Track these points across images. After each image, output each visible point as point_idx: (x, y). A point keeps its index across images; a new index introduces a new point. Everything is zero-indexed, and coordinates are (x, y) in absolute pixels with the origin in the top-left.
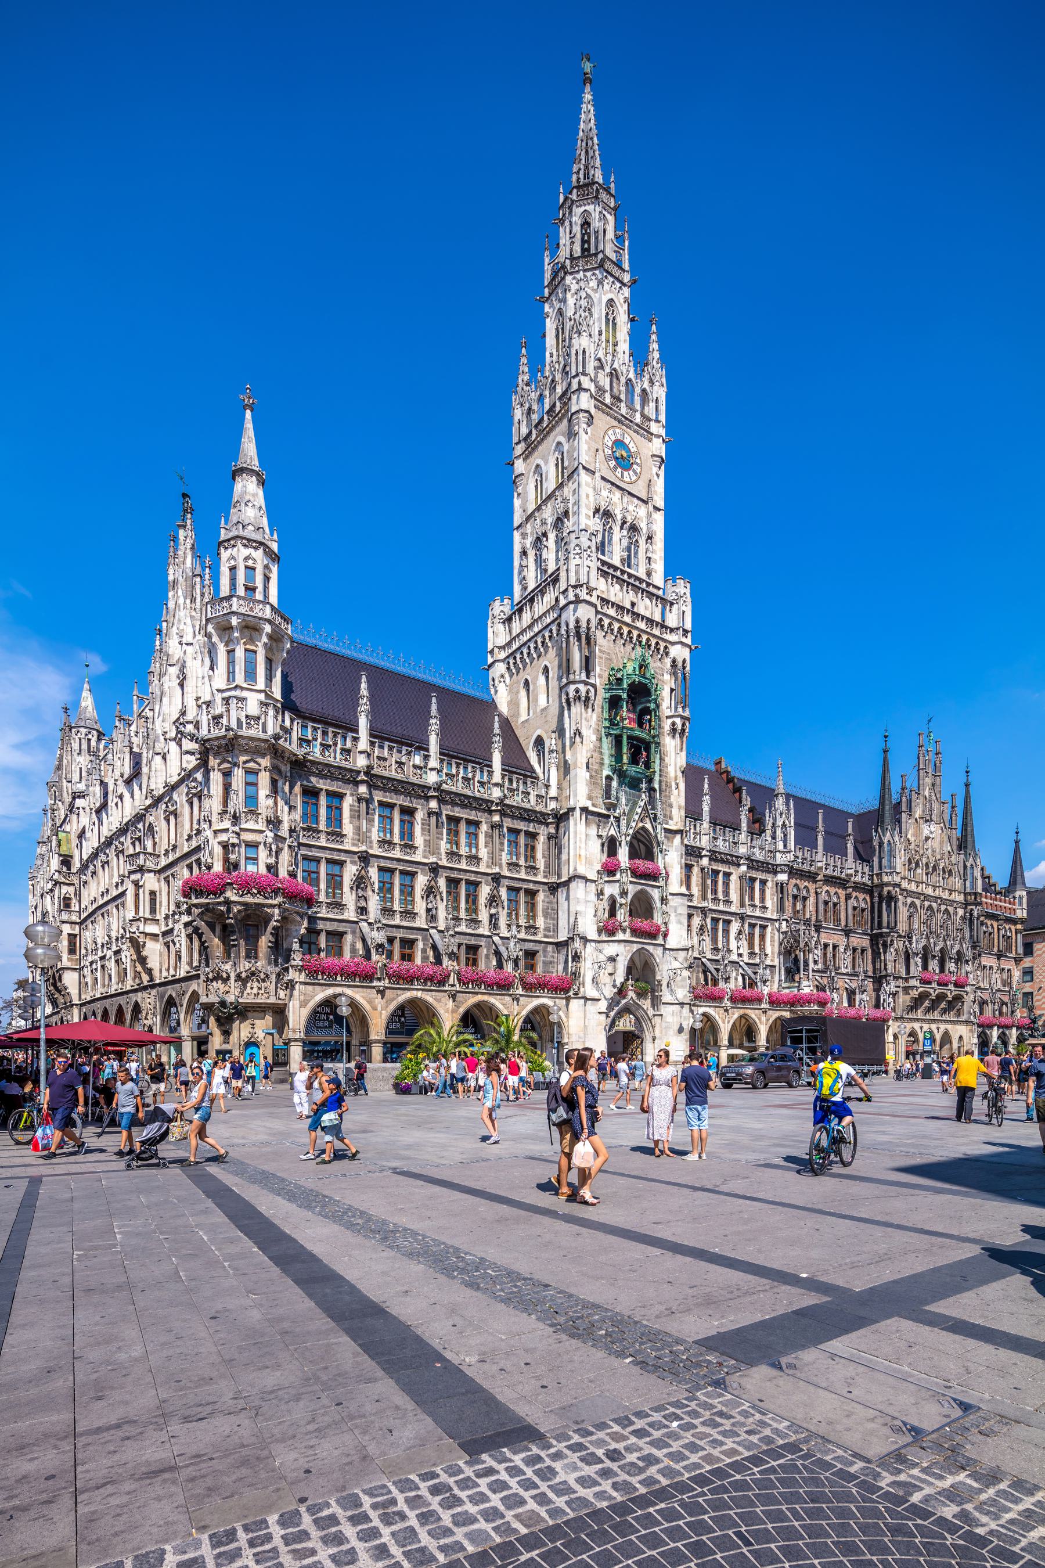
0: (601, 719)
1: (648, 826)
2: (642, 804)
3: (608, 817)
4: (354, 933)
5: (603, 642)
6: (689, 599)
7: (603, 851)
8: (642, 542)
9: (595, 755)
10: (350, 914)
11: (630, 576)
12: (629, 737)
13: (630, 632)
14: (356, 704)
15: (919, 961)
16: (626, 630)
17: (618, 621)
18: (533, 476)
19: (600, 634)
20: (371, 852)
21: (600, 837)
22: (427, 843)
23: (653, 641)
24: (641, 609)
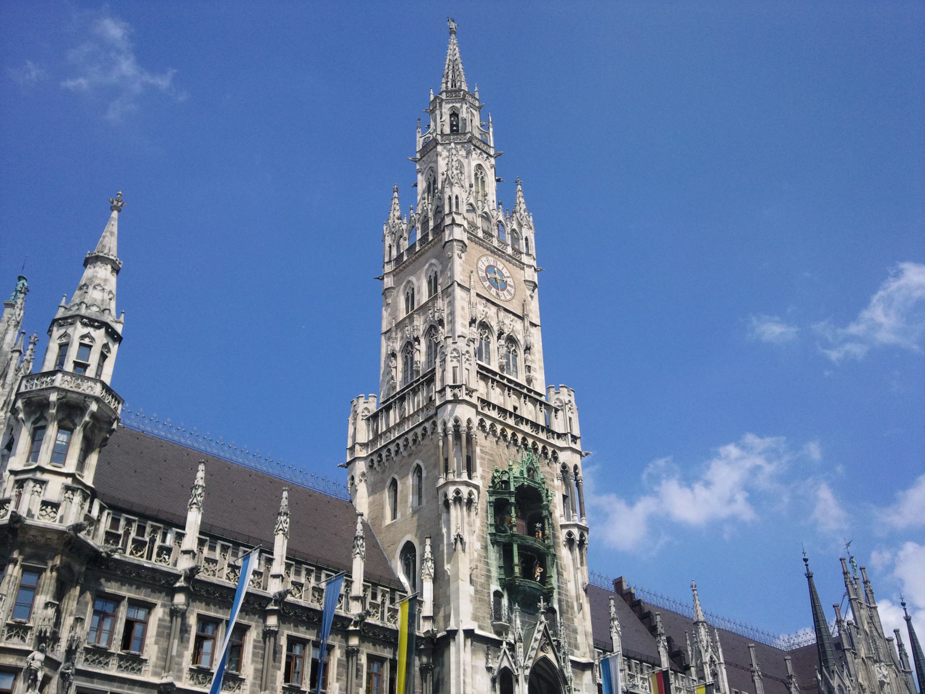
1: (551, 656)
2: (542, 628)
3: (501, 643)
5: (483, 444)
6: (575, 407)
7: (494, 687)
8: (521, 352)
9: (481, 565)
11: (510, 381)
13: (514, 435)
16: (509, 432)
17: (501, 423)
20: (179, 685)
21: (489, 669)
23: (540, 446)
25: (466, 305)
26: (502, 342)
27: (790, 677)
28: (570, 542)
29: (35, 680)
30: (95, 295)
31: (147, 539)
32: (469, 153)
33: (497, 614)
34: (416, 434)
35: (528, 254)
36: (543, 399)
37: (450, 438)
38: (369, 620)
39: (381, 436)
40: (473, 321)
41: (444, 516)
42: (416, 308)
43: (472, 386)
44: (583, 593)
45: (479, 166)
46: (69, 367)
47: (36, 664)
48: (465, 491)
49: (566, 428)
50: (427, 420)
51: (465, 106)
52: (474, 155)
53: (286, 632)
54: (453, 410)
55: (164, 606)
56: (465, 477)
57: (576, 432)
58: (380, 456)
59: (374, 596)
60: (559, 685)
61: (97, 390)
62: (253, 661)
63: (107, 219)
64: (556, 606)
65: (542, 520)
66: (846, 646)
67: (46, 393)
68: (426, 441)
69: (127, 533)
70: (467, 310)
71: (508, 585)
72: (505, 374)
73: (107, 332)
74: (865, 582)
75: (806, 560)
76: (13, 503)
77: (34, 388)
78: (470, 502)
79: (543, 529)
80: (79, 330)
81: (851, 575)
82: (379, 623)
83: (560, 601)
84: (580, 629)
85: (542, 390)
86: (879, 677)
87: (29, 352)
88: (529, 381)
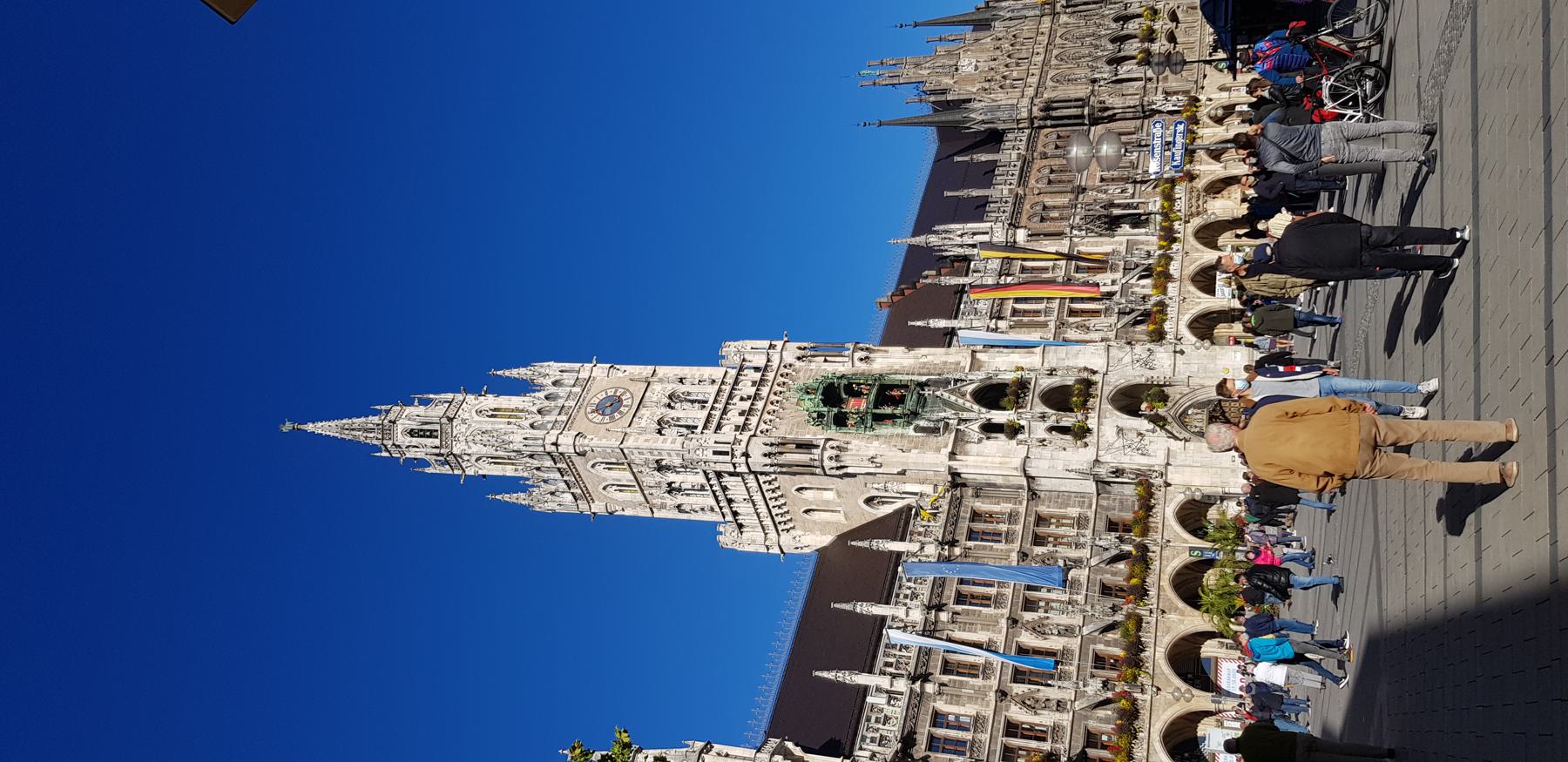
1: (970, 388)
2: (946, 395)
4: (1086, 718)
5: (783, 430)
8: (681, 389)
10: (1065, 719)
11: (715, 401)
14: (843, 685)
16: (770, 407)
18: (614, 497)
19: (775, 433)
21: (980, 440)
22: (985, 627)
24: (752, 391)
25: (642, 438)
33: (934, 431)
36: (733, 372)
40: (660, 432)
45: (479, 412)
56: (817, 451)
66: (942, 98)
70: (648, 436)
72: (709, 405)
84: (944, 359)
85: (721, 371)
86: (970, 69)
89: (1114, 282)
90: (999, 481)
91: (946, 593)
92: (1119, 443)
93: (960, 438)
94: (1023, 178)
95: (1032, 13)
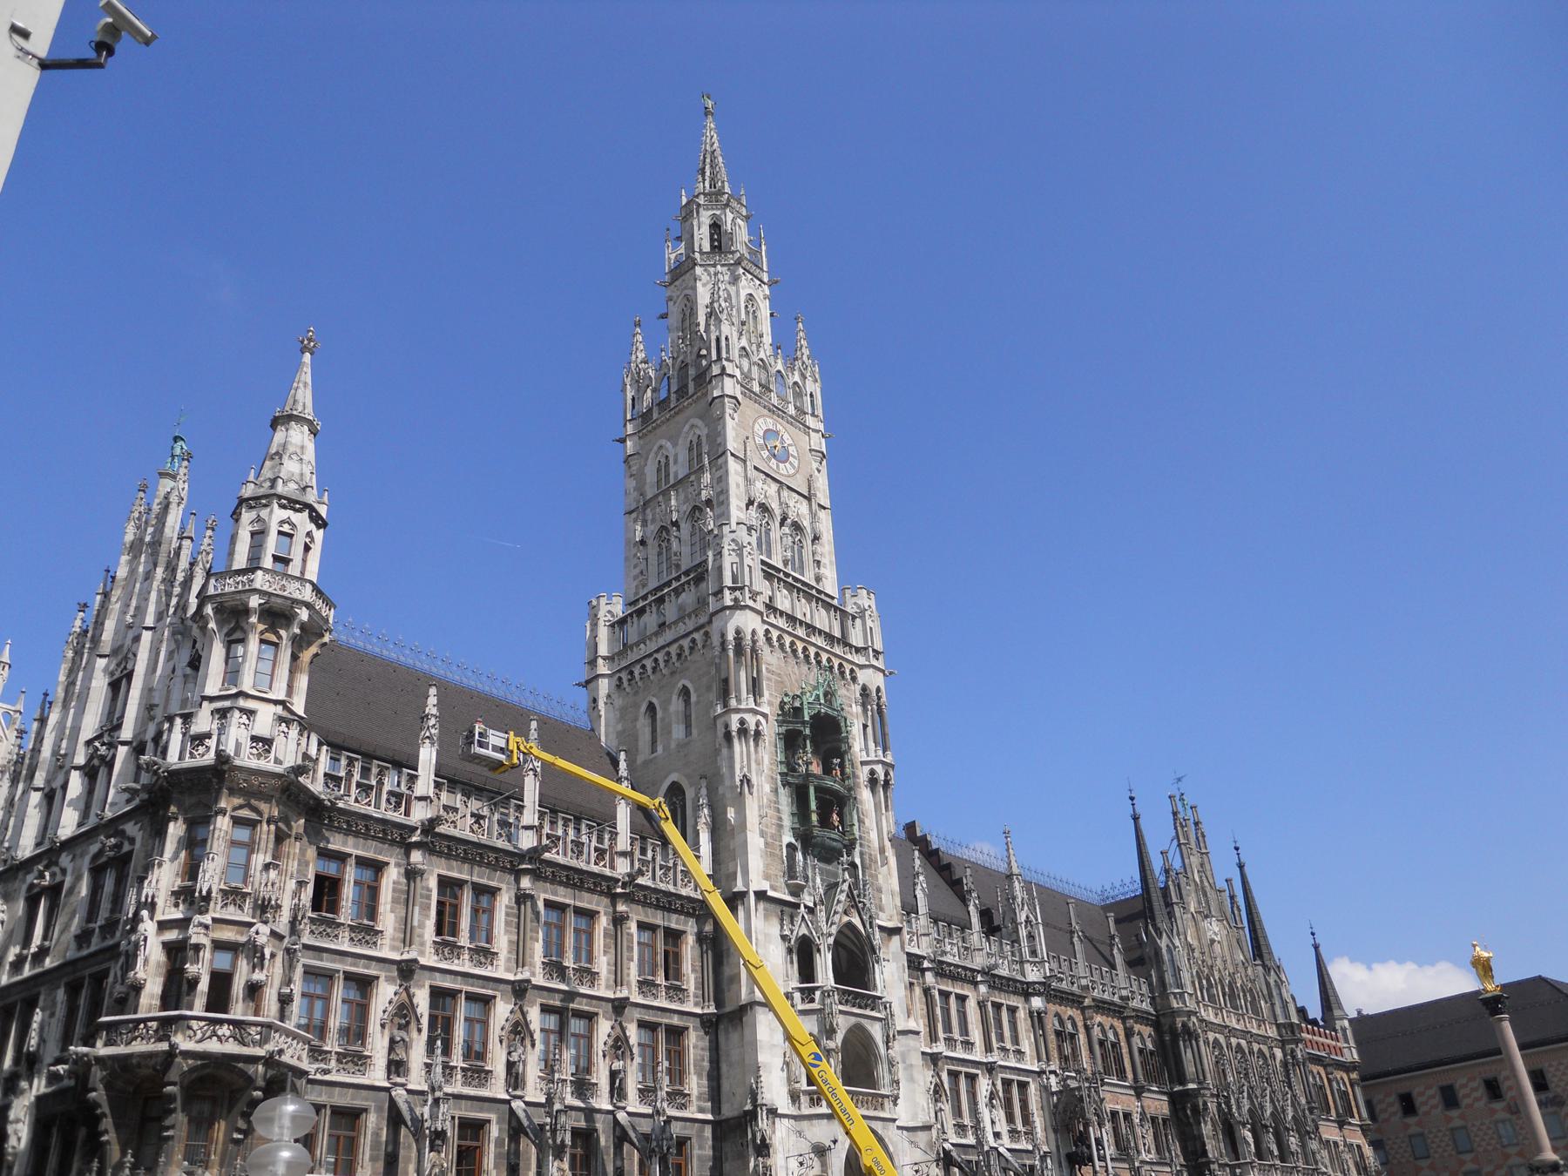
0: (774, 762)
1: (856, 921)
2: (845, 887)
3: (797, 906)
4: (379, 1110)
5: (771, 659)
6: (875, 614)
9: (771, 812)
10: (377, 1075)
11: (795, 579)
12: (817, 789)
13: (805, 649)
15: (1249, 1135)
16: (800, 646)
17: (790, 634)
20: (423, 961)
21: (784, 938)
25: (741, 480)
26: (786, 530)
27: (1112, 937)
28: (873, 781)
29: (262, 957)
30: (290, 467)
31: (374, 783)
32: (735, 280)
33: (791, 872)
34: (681, 648)
35: (813, 415)
36: (835, 602)
37: (731, 654)
38: (640, 881)
39: (631, 648)
40: (750, 503)
41: (725, 751)
42: (672, 481)
43: (756, 588)
44: (888, 844)
46: (268, 562)
47: (262, 940)
48: (751, 720)
49: (866, 641)
50: (697, 629)
51: (730, 216)
52: (743, 282)
53: (543, 896)
54: (731, 616)
55: (398, 865)
57: (879, 646)
58: (631, 673)
59: (643, 851)
60: (864, 954)
61: (307, 594)
62: (507, 932)
63: (299, 365)
64: (858, 861)
65: (841, 755)
67: (243, 596)
68: (696, 656)
69: (350, 774)
70: (742, 488)
71: (805, 839)
73: (311, 517)
74: (1196, 824)
75: (1132, 799)
76: (215, 738)
77: (227, 589)
78: (758, 734)
79: (842, 766)
80: (277, 515)
81: (1180, 816)
82: (650, 883)
83: (862, 854)
87: (206, 541)
88: (818, 579)
89: (997, 1135)
90: (727, 971)
91: (561, 890)
92: (805, 1147)
93: (787, 910)
94: (1102, 1006)
95: (1278, 1011)
